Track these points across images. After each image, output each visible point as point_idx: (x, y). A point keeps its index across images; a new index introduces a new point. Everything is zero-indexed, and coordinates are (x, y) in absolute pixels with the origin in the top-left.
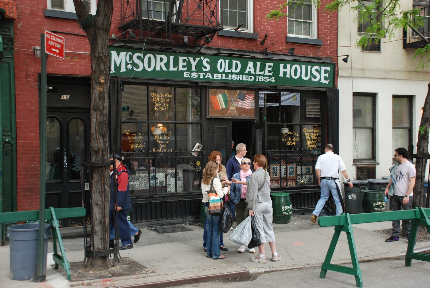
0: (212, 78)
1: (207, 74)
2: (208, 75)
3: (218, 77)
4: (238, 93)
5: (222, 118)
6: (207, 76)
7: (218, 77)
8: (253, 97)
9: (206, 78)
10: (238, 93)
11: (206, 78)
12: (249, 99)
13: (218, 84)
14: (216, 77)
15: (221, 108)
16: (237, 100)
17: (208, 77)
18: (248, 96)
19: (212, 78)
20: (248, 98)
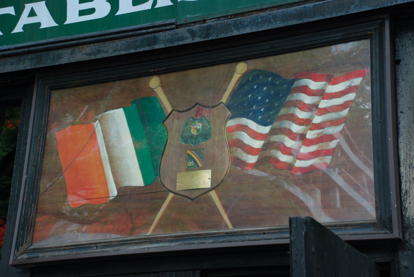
0: (54, 24)
1: (28, 8)
2: (32, 13)
3: (92, 11)
4: (236, 77)
5: (111, 252)
6: (25, 20)
7: (92, 11)
8: (357, 81)
9: (18, 29)
10: (236, 77)
11: (18, 29)
12: (324, 104)
13: (88, 49)
14: (82, 13)
15: (114, 192)
16: (231, 123)
17: (33, 20)
18: (314, 85)
19: (54, 24)
20: (322, 94)
